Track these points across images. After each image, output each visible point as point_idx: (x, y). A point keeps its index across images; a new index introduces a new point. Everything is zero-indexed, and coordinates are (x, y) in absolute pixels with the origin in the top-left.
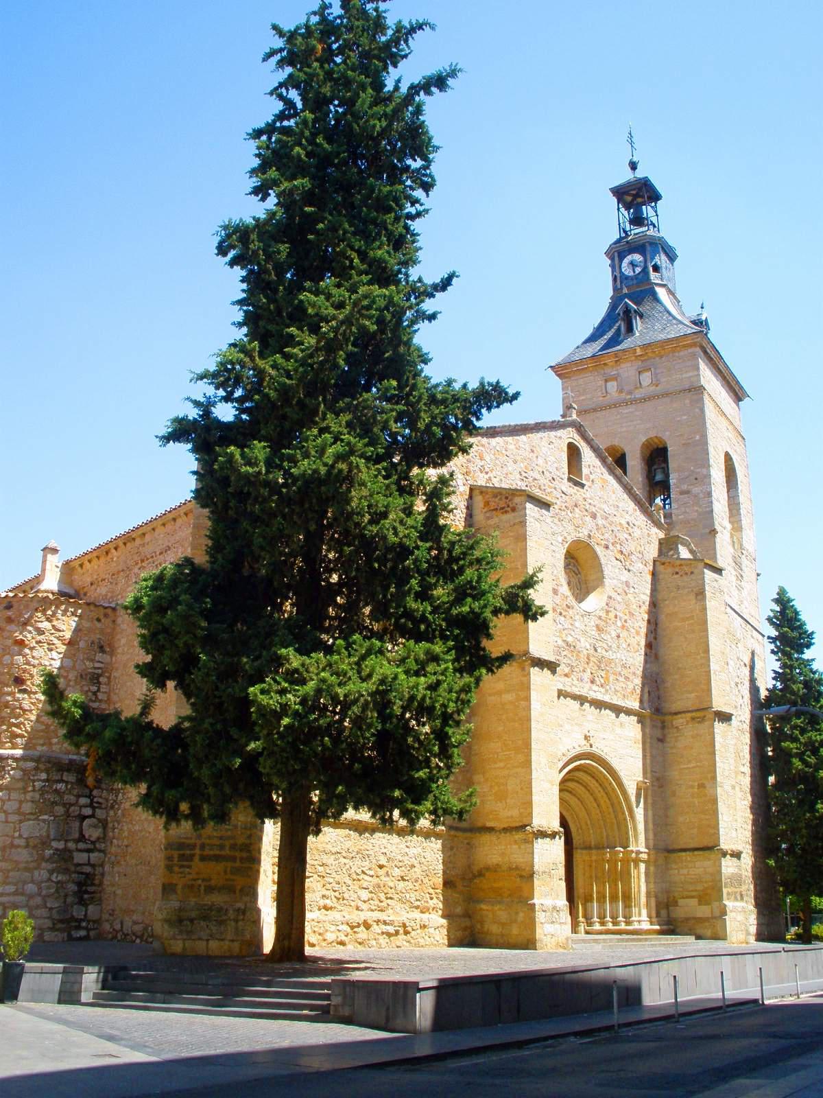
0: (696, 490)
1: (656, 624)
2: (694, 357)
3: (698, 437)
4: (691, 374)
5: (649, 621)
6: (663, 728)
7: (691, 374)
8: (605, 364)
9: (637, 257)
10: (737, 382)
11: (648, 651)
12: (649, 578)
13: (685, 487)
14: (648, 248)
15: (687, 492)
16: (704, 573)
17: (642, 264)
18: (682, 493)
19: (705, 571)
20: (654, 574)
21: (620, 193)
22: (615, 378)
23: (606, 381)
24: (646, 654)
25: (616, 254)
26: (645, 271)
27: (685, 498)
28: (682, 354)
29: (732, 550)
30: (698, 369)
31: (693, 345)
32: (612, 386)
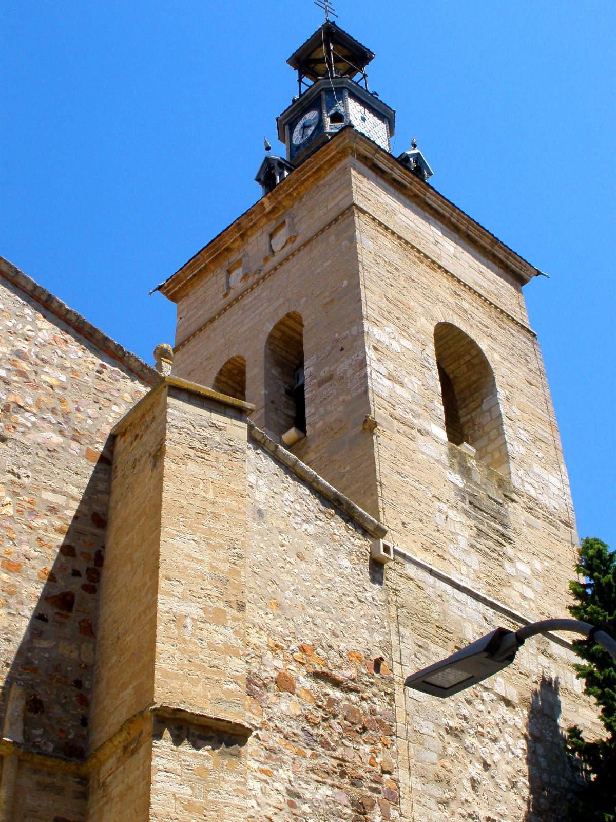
0: (343, 367)
1: (99, 559)
2: (345, 172)
3: (345, 283)
4: (341, 197)
5: (66, 550)
6: (84, 796)
7: (341, 197)
8: (228, 249)
9: (312, 116)
10: (495, 241)
11: (50, 611)
12: (88, 468)
13: (323, 373)
14: (324, 96)
15: (330, 378)
16: (166, 406)
17: (316, 121)
18: (320, 384)
19: (170, 400)
20: (106, 461)
21: (304, 61)
22: (239, 263)
23: (229, 272)
24: (39, 617)
25: (287, 127)
26: (320, 125)
27: (327, 389)
28: (329, 177)
29: (457, 479)
30: (349, 184)
31: (343, 153)
32: (238, 274)
